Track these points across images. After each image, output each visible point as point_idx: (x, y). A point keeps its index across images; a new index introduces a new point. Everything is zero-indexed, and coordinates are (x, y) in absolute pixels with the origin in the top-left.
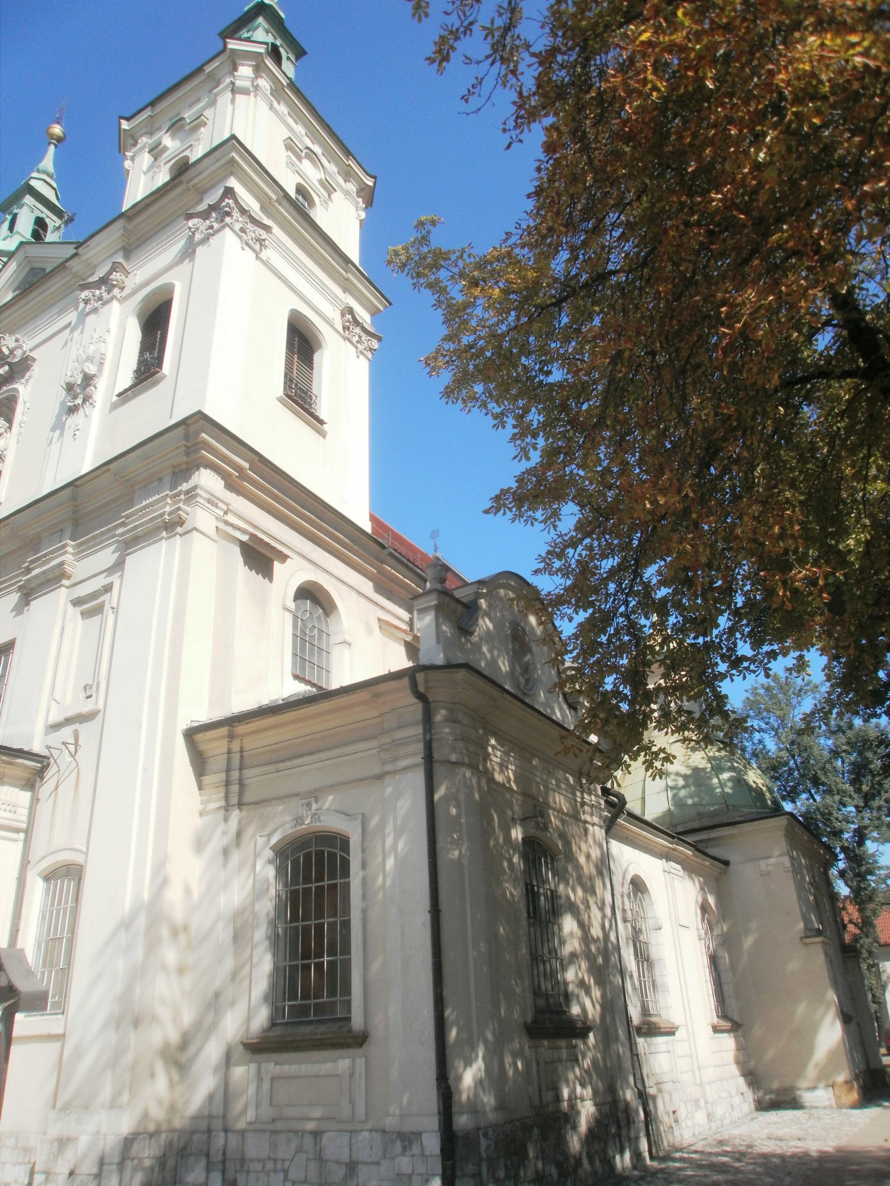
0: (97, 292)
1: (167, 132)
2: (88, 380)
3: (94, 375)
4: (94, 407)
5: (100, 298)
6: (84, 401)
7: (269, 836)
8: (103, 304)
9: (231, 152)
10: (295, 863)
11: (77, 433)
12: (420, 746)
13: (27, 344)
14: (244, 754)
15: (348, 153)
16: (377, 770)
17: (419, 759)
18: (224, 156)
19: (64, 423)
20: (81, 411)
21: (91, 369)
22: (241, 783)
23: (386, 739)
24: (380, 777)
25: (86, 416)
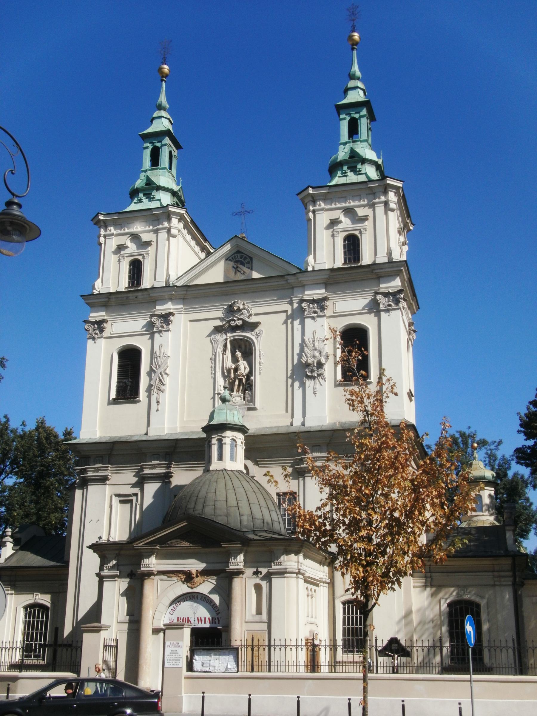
0: (311, 306)
1: (342, 212)
2: (320, 365)
3: (324, 364)
4: (325, 381)
5: (315, 312)
6: (319, 375)
7: (446, 599)
8: (318, 316)
9: (402, 266)
10: (456, 610)
11: (316, 392)
12: (511, 579)
13: (254, 311)
14: (431, 567)
15: (409, 216)
16: (492, 583)
17: (510, 583)
18: (397, 267)
19: (305, 382)
20: (316, 380)
21: (323, 361)
22: (431, 577)
23: (496, 574)
24: (494, 585)
25: (321, 385)
